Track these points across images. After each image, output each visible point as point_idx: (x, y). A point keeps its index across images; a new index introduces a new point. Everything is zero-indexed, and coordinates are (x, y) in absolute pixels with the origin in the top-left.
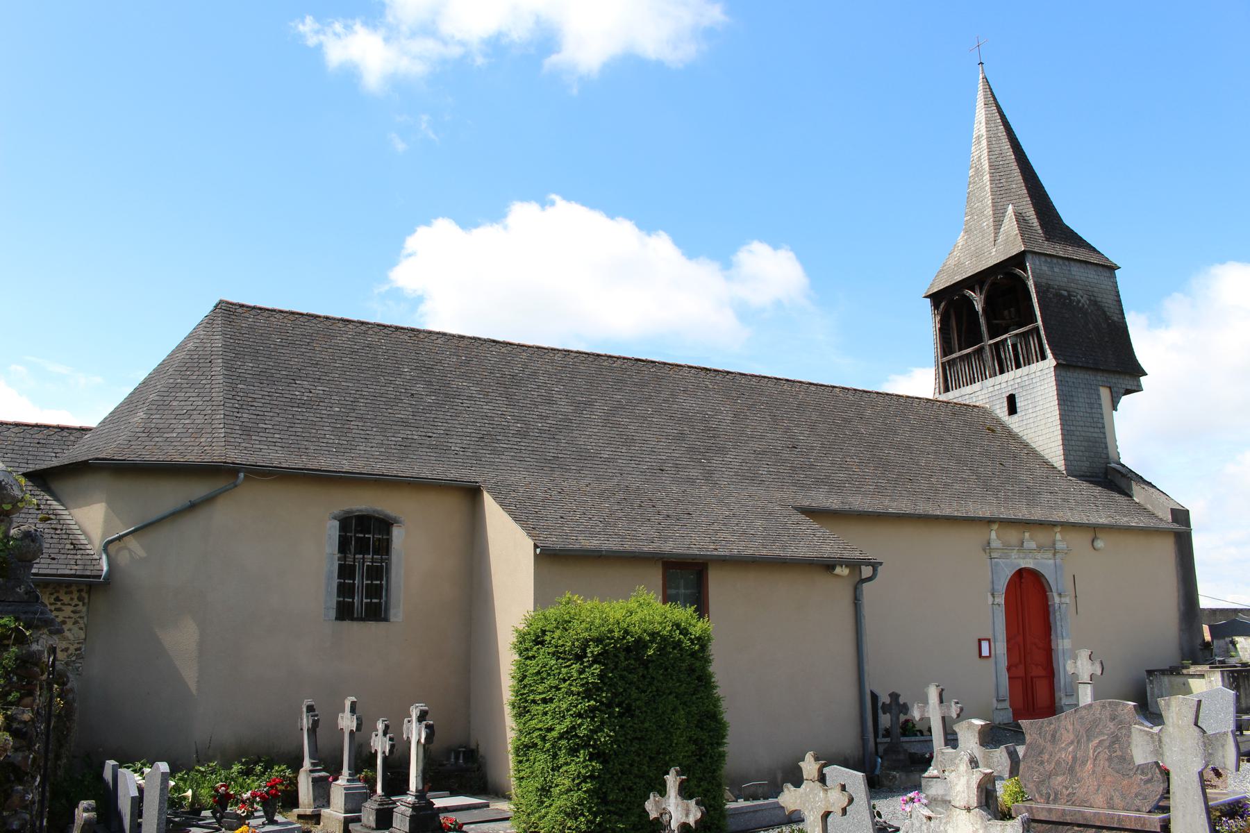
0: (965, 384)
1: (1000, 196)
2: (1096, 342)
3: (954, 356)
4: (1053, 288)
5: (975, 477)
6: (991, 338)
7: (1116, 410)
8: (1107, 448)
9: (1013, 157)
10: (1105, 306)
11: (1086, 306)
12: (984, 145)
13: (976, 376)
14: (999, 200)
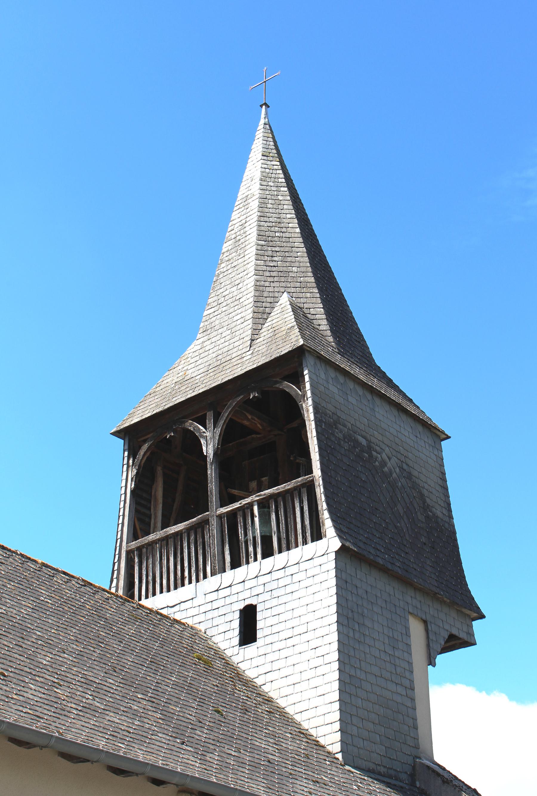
0: (165, 589)
1: (269, 279)
2: (407, 537)
3: (151, 537)
4: (345, 426)
5: (159, 716)
6: (223, 502)
7: (434, 666)
8: (416, 728)
9: (298, 230)
10: (424, 488)
11: (394, 475)
12: (251, 240)
13: (186, 574)
14: (267, 284)
